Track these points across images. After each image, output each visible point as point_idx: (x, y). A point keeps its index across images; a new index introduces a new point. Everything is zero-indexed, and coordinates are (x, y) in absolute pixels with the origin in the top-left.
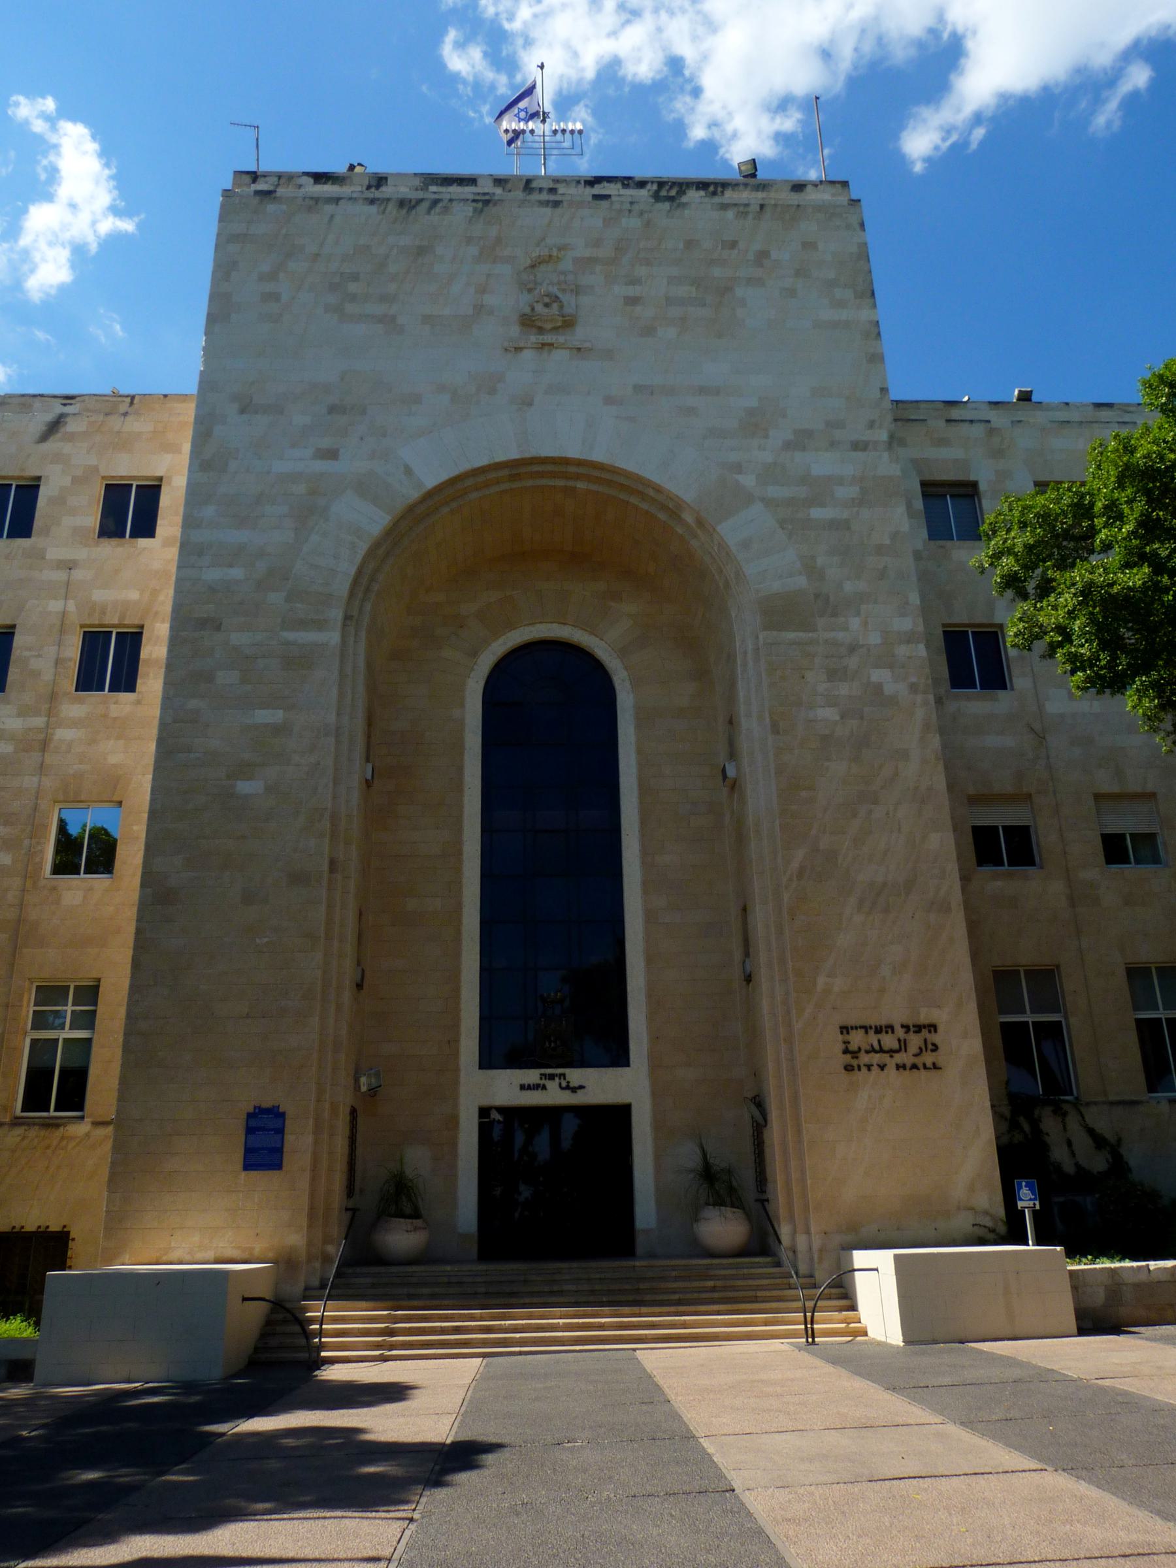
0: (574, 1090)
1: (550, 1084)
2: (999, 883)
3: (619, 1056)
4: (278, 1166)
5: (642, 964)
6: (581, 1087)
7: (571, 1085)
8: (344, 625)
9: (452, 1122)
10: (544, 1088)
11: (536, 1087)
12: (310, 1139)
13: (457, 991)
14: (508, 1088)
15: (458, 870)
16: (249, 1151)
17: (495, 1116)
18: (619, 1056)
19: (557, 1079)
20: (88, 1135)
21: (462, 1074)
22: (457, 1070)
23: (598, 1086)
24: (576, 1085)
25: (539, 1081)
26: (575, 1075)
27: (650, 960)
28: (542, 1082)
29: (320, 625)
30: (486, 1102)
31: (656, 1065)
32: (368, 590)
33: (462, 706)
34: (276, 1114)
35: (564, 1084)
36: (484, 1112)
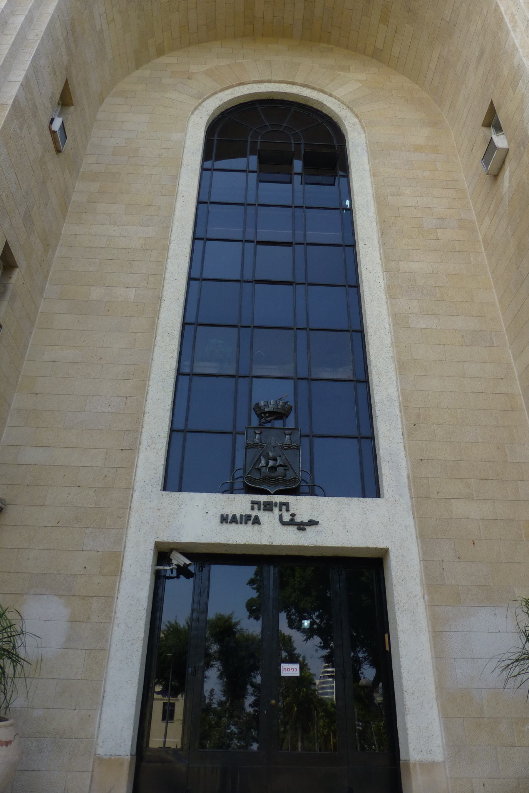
0: (301, 526)
1: (264, 516)
3: (367, 484)
5: (393, 374)
6: (313, 523)
7: (298, 519)
9: (113, 563)
10: (257, 521)
14: (202, 518)
15: (162, 264)
18: (367, 484)
19: (276, 510)
21: (136, 495)
22: (130, 488)
24: (306, 520)
25: (248, 512)
26: (302, 506)
27: (402, 367)
28: (253, 514)
30: (166, 537)
31: (421, 496)
33: (184, 130)
35: (287, 518)
36: (163, 554)
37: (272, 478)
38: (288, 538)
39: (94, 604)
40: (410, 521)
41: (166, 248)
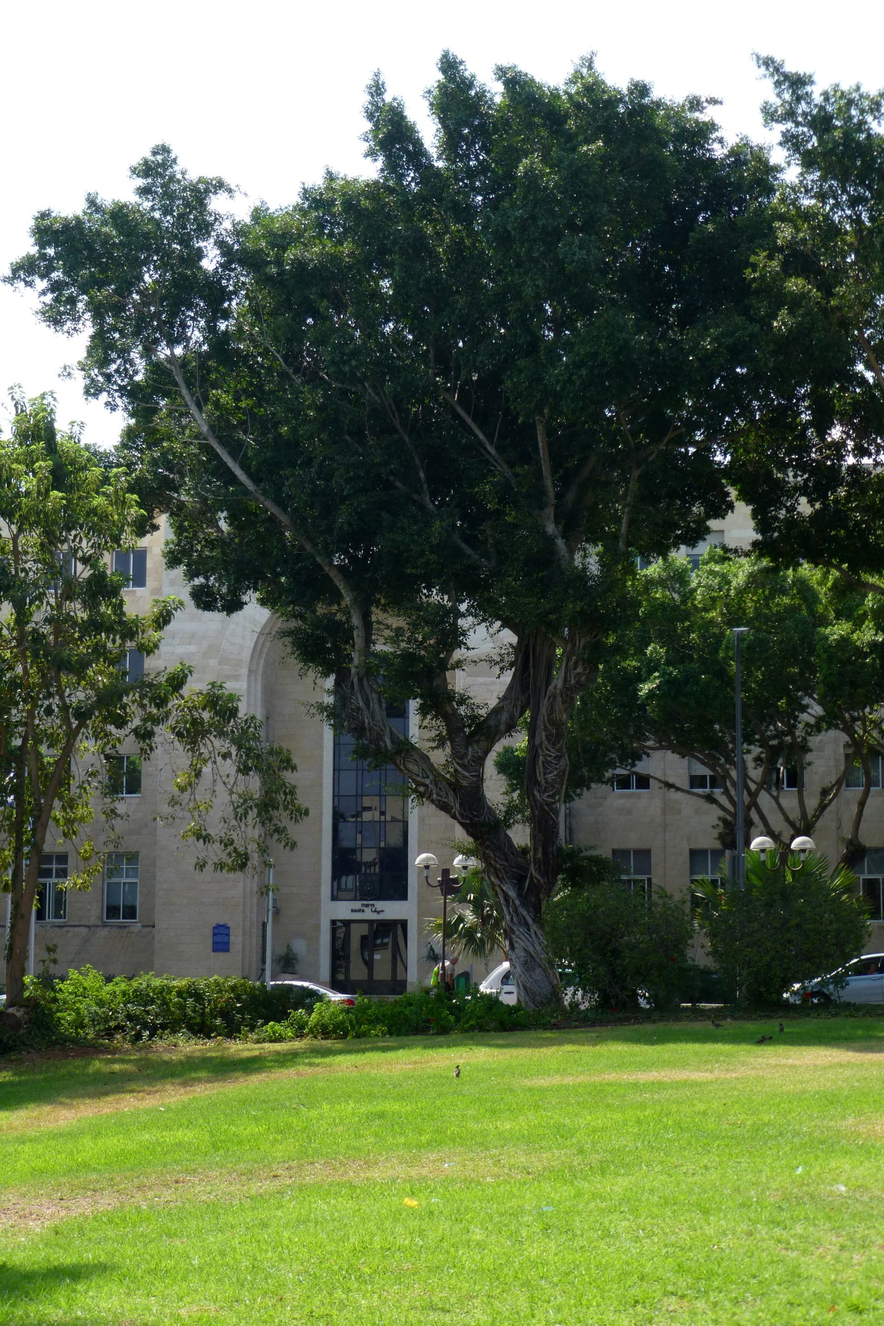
0: (378, 912)
1: (366, 909)
2: (623, 801)
3: (403, 895)
4: (227, 950)
8: (249, 676)
9: (317, 928)
11: (359, 910)
12: (240, 938)
13: (320, 859)
14: (344, 910)
15: (320, 794)
16: (214, 943)
17: (339, 924)
18: (403, 895)
20: (140, 932)
22: (319, 901)
23: (391, 910)
26: (379, 905)
29: (236, 678)
31: (420, 900)
32: (261, 651)
34: (226, 927)
36: (333, 922)
37: (371, 892)
38: (375, 916)
39: (313, 939)
40: (415, 909)
41: (321, 785)
